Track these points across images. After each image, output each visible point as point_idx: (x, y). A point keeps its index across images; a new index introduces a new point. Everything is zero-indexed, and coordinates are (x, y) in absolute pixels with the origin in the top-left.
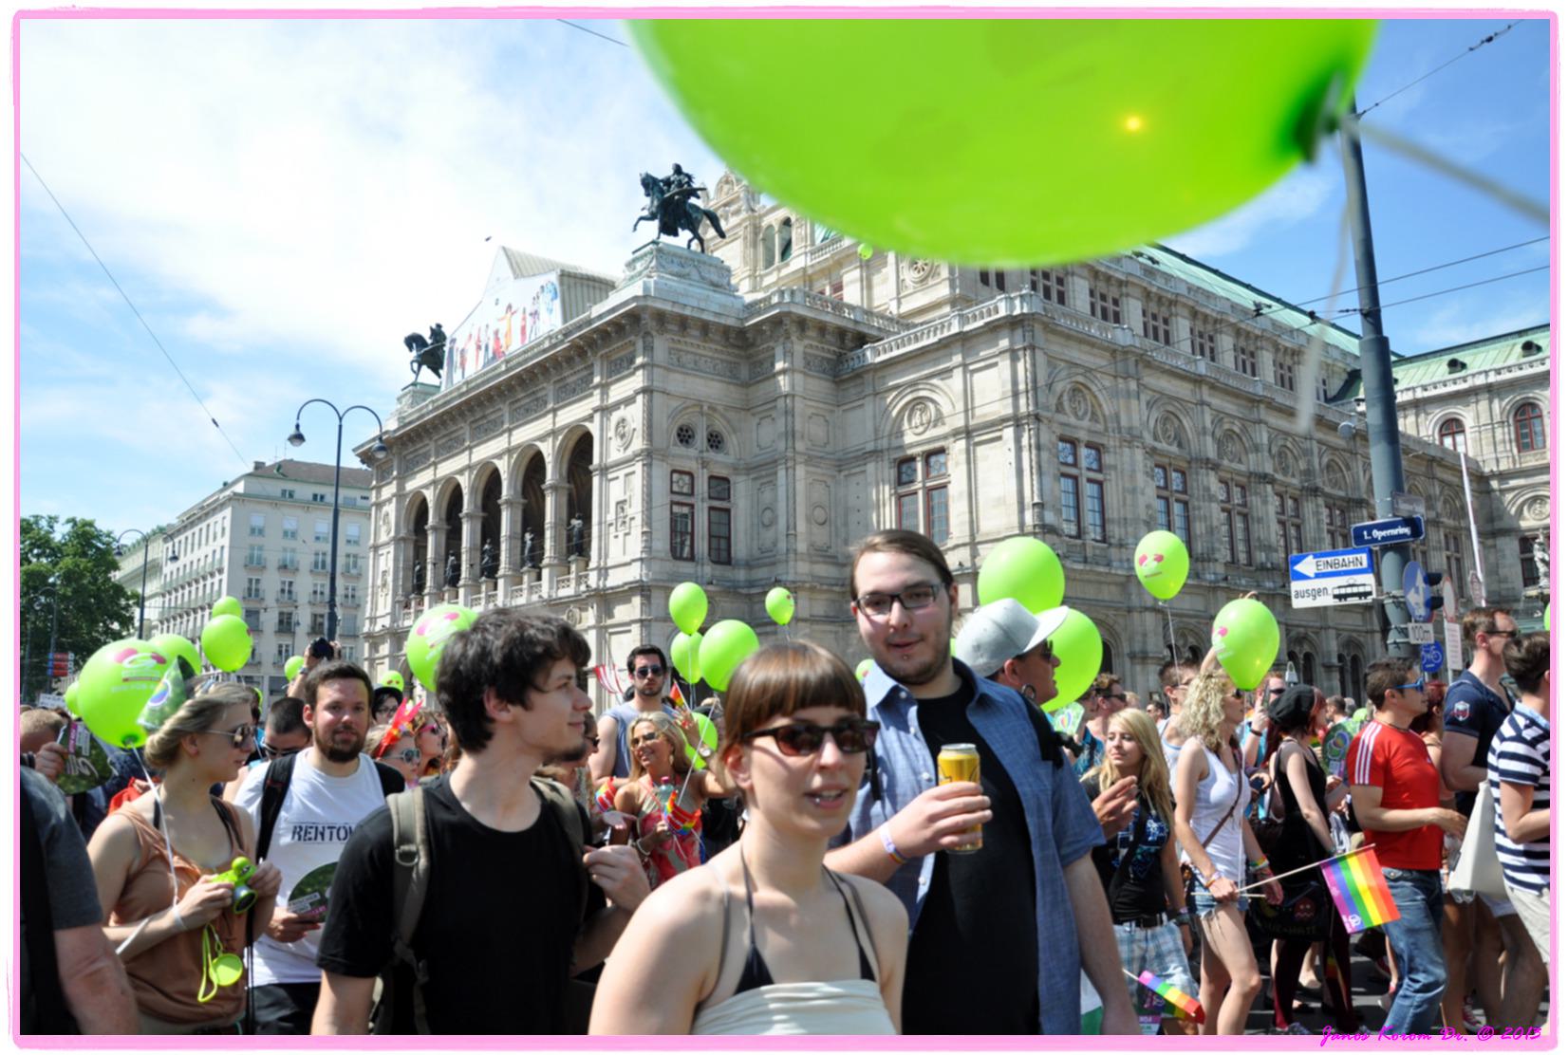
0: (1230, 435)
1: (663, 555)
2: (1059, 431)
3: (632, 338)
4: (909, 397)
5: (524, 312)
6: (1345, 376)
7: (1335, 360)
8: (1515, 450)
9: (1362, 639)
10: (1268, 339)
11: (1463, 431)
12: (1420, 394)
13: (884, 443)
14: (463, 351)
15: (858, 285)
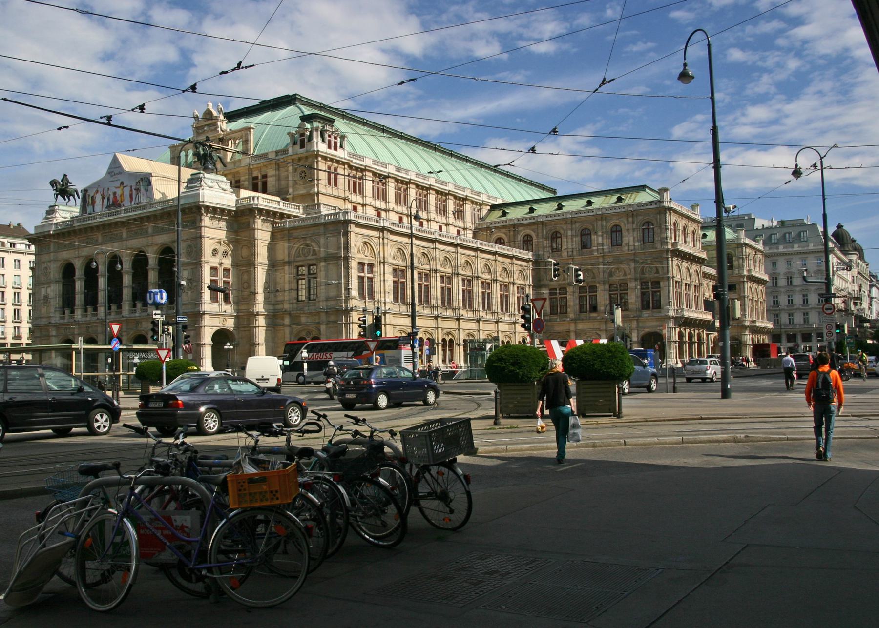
0: (424, 254)
1: (208, 302)
2: (358, 261)
3: (195, 215)
4: (303, 242)
5: (131, 187)
6: (488, 208)
7: (483, 201)
8: (551, 251)
9: (475, 333)
10: (452, 195)
11: (532, 240)
12: (516, 222)
13: (292, 259)
14: (93, 197)
15: (274, 178)
